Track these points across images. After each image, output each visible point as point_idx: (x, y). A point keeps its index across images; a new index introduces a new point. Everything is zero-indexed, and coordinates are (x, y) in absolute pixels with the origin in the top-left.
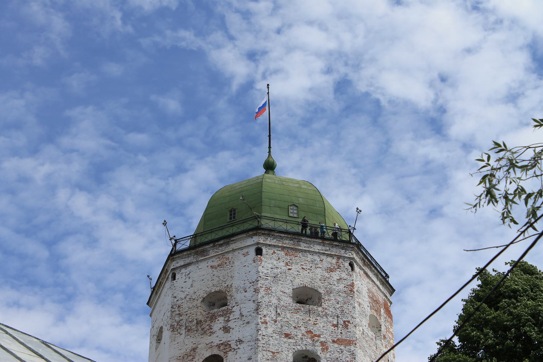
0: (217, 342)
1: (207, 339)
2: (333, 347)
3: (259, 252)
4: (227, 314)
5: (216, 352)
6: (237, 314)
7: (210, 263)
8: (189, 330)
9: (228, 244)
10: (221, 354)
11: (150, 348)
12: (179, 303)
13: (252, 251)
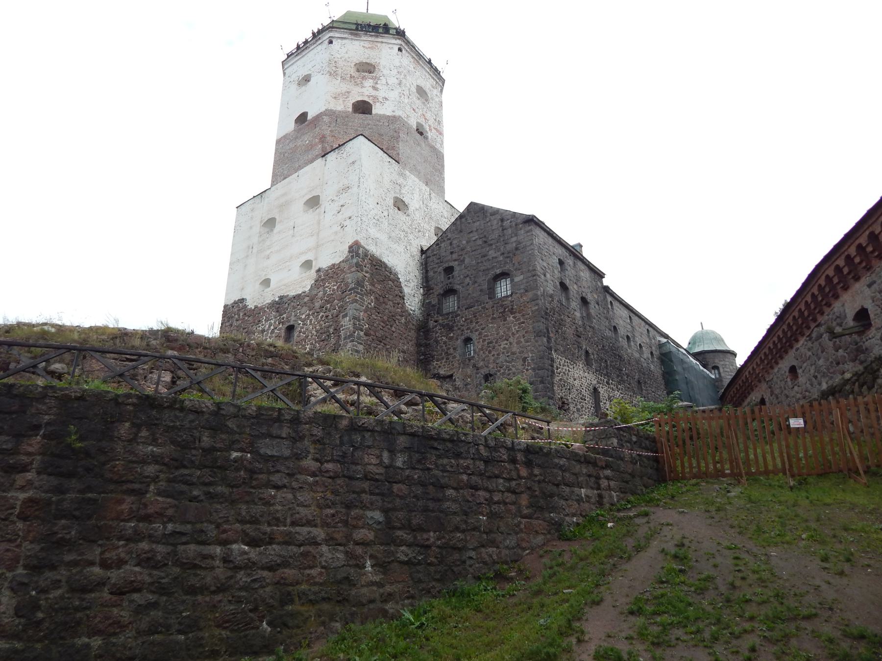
0: (367, 93)
1: (358, 89)
2: (434, 131)
3: (400, 50)
4: (376, 79)
5: (366, 99)
6: (384, 81)
7: (362, 43)
8: (343, 79)
9: (377, 36)
10: (371, 102)
11: (284, 90)
12: (336, 59)
13: (396, 48)
